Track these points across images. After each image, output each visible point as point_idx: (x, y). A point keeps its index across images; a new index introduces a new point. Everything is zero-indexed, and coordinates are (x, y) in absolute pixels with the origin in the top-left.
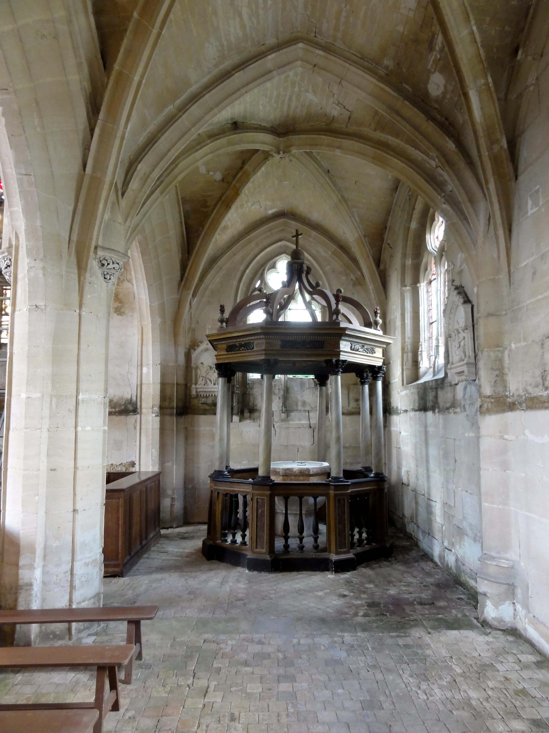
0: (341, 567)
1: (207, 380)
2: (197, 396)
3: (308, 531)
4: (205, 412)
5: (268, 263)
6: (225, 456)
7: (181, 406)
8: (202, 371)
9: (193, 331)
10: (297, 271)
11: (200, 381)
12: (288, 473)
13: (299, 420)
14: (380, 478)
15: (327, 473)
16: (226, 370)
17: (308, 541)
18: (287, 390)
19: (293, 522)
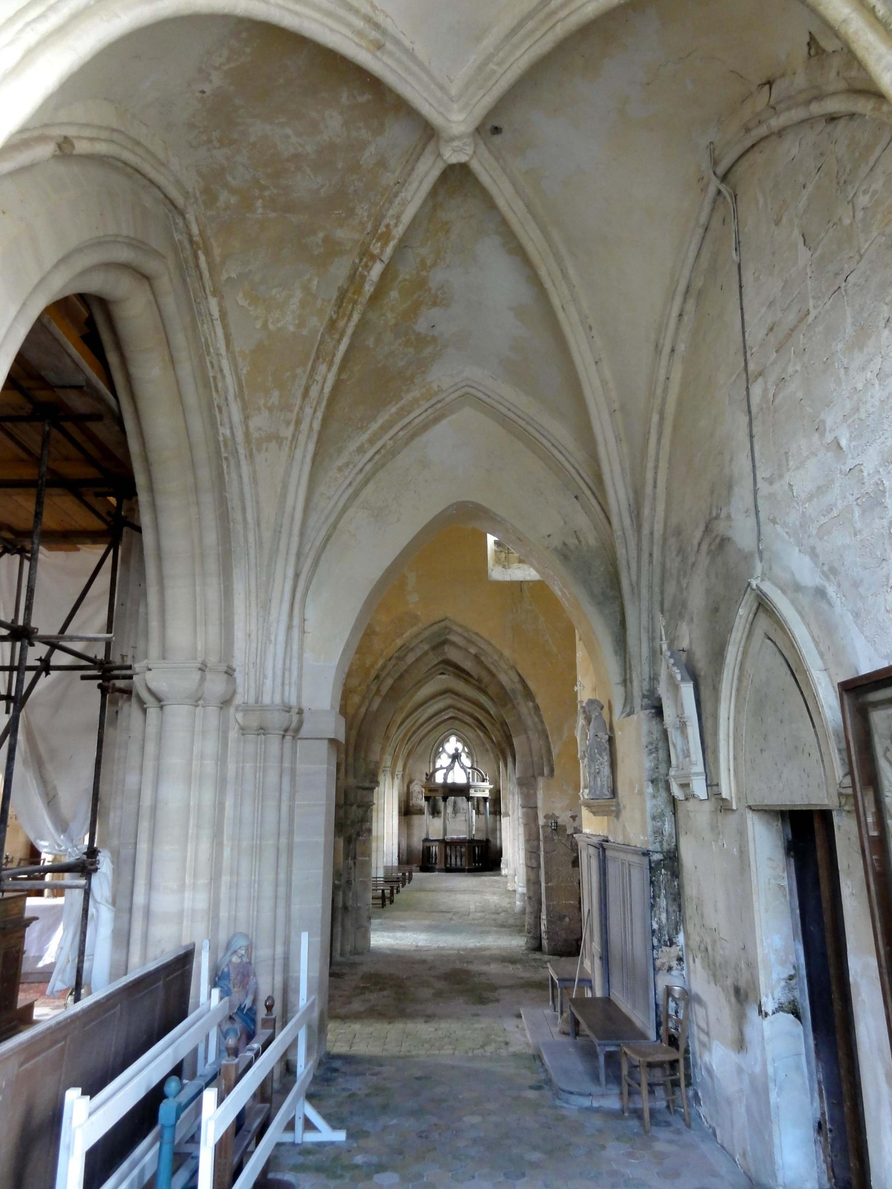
0: (470, 871)
1: (417, 798)
2: (413, 806)
3: (458, 859)
4: (416, 814)
5: (446, 739)
6: (427, 834)
7: (407, 811)
8: (415, 794)
9: (410, 774)
10: (456, 757)
11: (414, 799)
12: (452, 839)
13: (461, 817)
14: (488, 841)
15: (465, 839)
16: (427, 799)
17: (459, 863)
18: (455, 803)
19: (453, 858)
